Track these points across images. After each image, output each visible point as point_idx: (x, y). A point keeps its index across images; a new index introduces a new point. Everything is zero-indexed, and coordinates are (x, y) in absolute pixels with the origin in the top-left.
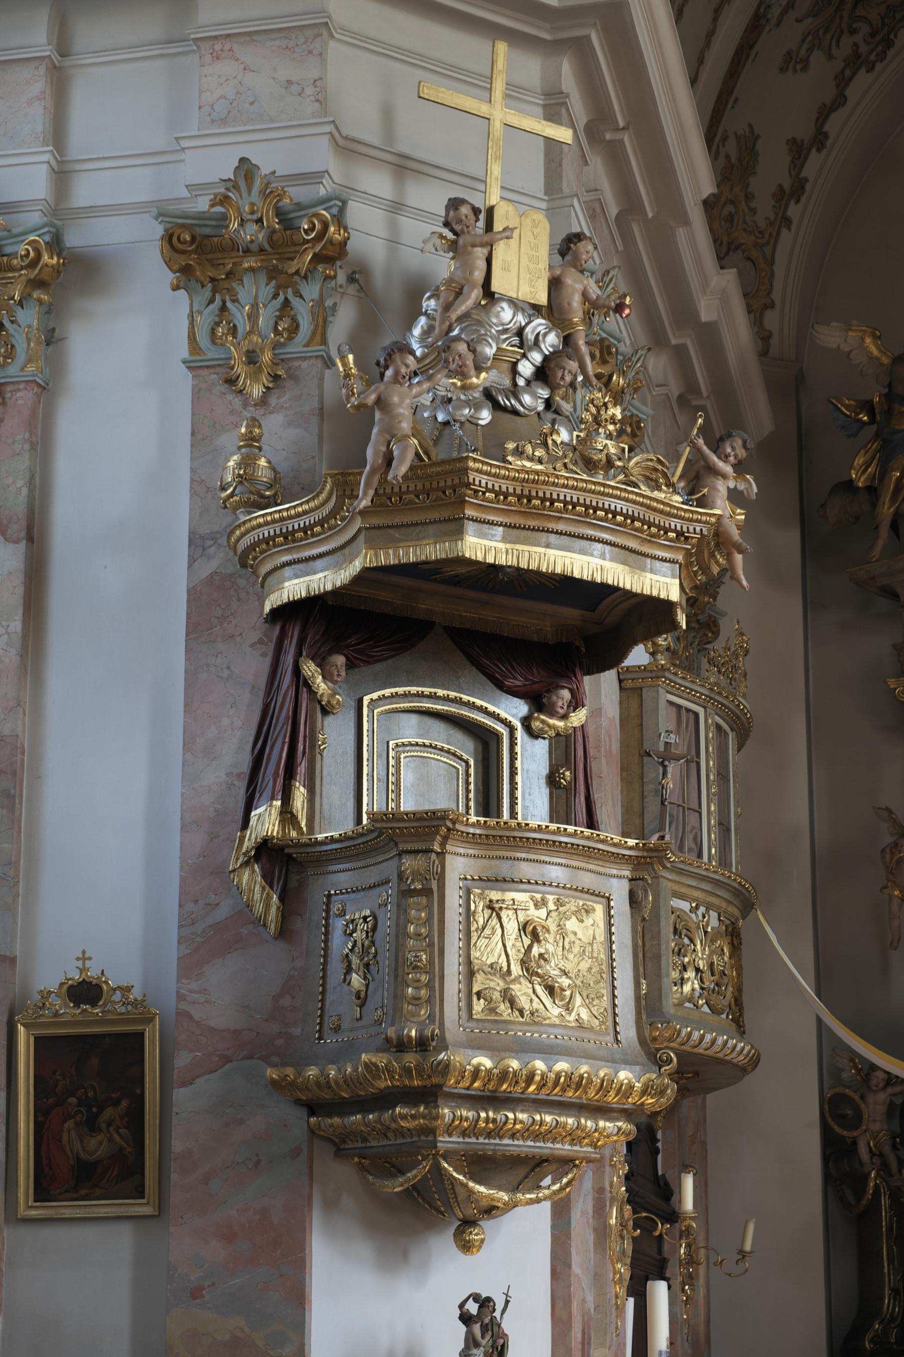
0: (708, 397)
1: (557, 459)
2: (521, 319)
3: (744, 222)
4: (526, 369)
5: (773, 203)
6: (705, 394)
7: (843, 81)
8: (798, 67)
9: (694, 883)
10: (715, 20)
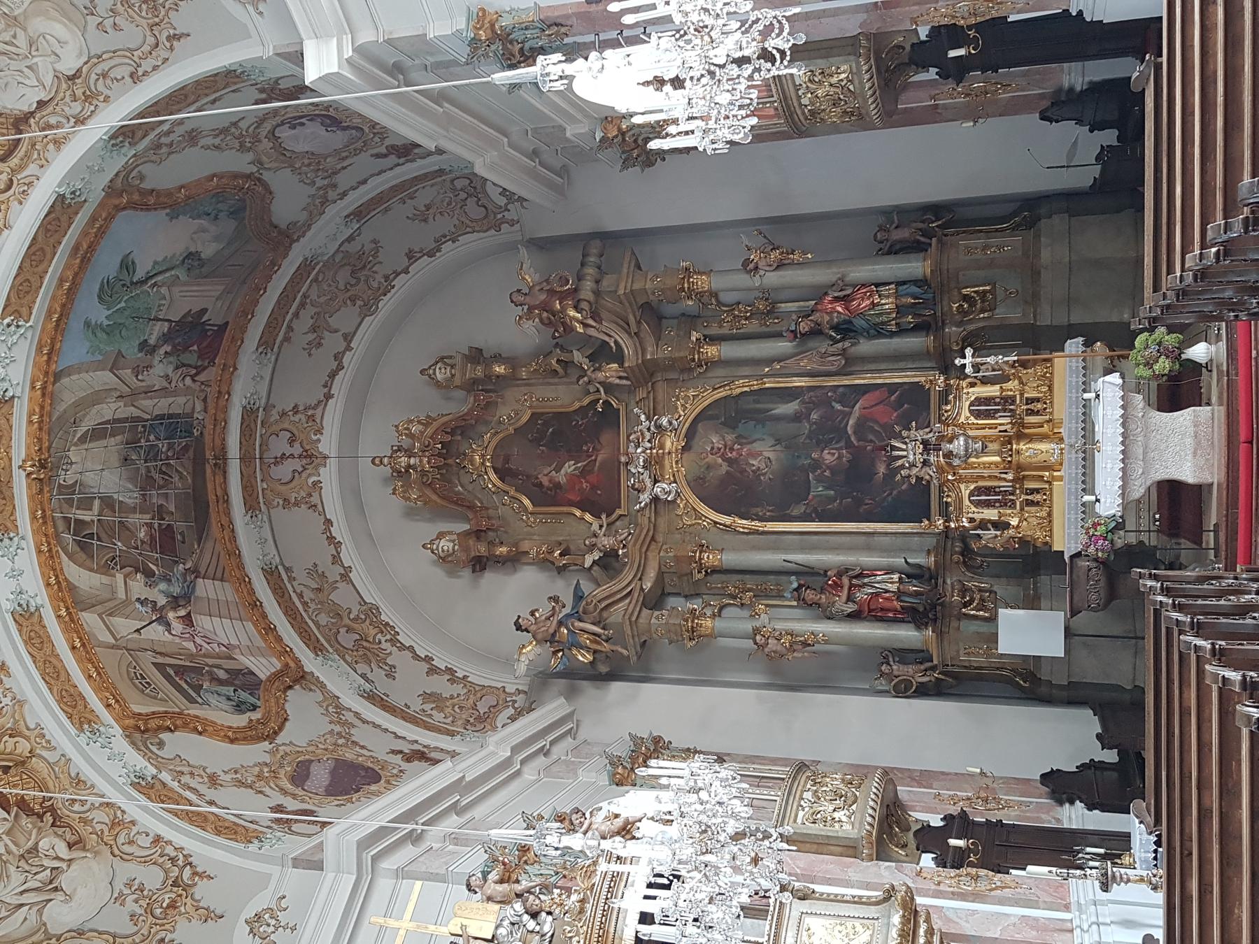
1: (578, 931)
2: (506, 923)
4: (531, 925)
7: (403, 647)
9: (789, 808)
10: (368, 722)
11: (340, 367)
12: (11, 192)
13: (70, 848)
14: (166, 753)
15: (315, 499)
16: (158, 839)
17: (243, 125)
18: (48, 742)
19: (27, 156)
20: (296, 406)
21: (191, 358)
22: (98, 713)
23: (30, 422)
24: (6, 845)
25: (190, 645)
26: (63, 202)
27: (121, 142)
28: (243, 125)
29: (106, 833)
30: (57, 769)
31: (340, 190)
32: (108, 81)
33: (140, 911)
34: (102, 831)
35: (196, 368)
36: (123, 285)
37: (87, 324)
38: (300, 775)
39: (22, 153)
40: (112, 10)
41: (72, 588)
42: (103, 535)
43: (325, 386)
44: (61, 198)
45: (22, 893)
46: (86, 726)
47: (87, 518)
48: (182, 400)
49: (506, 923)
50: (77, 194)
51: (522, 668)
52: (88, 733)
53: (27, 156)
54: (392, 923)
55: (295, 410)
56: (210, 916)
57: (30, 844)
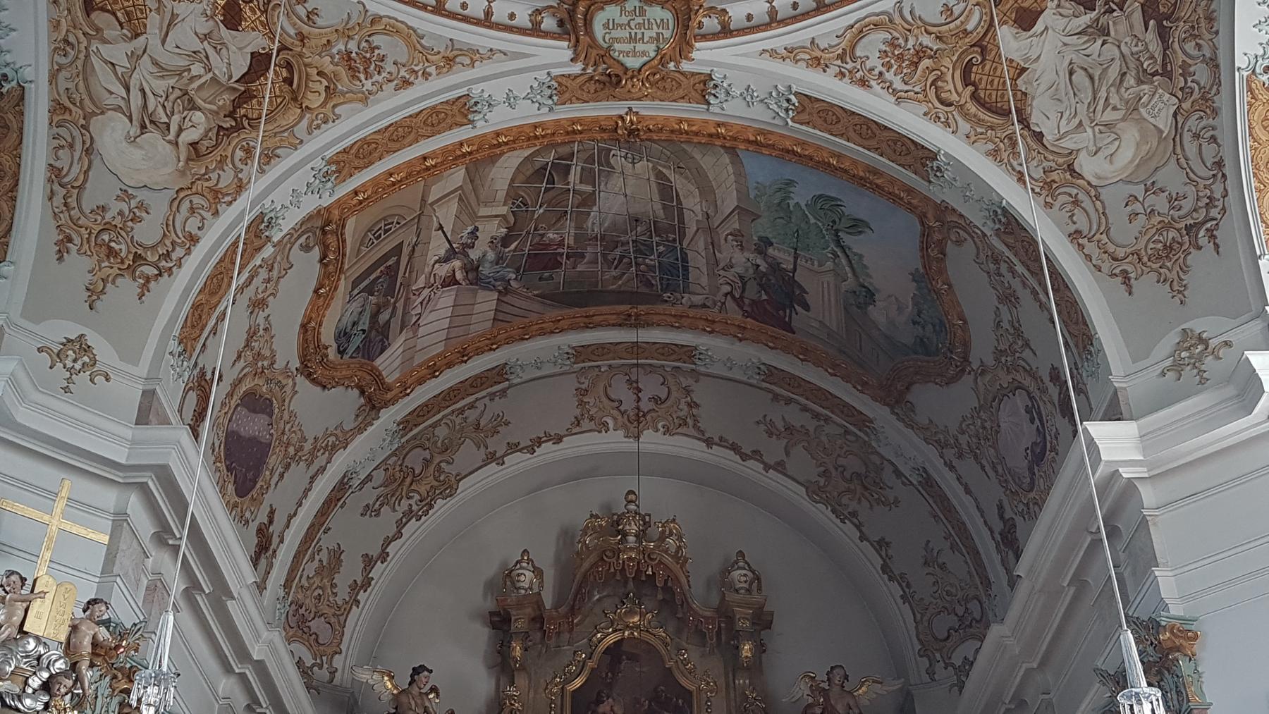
0: (267, 708)
3: (328, 600)
5: (349, 590)
6: (264, 706)
7: (401, 525)
8: (373, 514)
10: (311, 482)
11: (744, 457)
12: (938, 104)
13: (191, 144)
14: (296, 253)
15: (586, 424)
16: (194, 240)
17: (1027, 354)
18: (318, 127)
19: (979, 122)
20: (697, 405)
21: (752, 292)
22: (347, 181)
23: (680, 121)
24: (200, 77)
25: (421, 282)
26: (927, 158)
27: (1000, 221)
28: (1027, 354)
29: (206, 184)
30: (286, 134)
31: (955, 462)
32: (1069, 207)
33: (108, 216)
34: (207, 180)
35: (742, 297)
36: (834, 222)
37: (790, 183)
38: (255, 403)
39: (982, 116)
40: (1153, 210)
41: (493, 159)
42: (551, 194)
43: (721, 439)
44: (933, 156)
45: (143, 91)
46: (333, 168)
47: (571, 178)
48: (704, 281)
49: (41, 649)
50: (938, 174)
51: (364, 675)
52: (325, 169)
53: (979, 122)
54: (60, 505)
55: (693, 405)
56: (94, 294)
57: (200, 102)
